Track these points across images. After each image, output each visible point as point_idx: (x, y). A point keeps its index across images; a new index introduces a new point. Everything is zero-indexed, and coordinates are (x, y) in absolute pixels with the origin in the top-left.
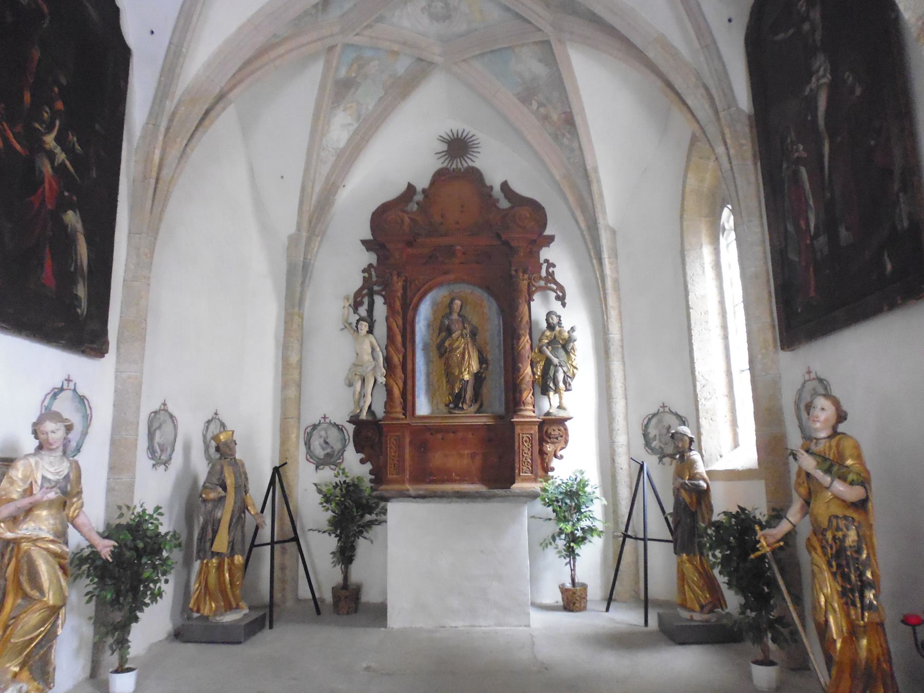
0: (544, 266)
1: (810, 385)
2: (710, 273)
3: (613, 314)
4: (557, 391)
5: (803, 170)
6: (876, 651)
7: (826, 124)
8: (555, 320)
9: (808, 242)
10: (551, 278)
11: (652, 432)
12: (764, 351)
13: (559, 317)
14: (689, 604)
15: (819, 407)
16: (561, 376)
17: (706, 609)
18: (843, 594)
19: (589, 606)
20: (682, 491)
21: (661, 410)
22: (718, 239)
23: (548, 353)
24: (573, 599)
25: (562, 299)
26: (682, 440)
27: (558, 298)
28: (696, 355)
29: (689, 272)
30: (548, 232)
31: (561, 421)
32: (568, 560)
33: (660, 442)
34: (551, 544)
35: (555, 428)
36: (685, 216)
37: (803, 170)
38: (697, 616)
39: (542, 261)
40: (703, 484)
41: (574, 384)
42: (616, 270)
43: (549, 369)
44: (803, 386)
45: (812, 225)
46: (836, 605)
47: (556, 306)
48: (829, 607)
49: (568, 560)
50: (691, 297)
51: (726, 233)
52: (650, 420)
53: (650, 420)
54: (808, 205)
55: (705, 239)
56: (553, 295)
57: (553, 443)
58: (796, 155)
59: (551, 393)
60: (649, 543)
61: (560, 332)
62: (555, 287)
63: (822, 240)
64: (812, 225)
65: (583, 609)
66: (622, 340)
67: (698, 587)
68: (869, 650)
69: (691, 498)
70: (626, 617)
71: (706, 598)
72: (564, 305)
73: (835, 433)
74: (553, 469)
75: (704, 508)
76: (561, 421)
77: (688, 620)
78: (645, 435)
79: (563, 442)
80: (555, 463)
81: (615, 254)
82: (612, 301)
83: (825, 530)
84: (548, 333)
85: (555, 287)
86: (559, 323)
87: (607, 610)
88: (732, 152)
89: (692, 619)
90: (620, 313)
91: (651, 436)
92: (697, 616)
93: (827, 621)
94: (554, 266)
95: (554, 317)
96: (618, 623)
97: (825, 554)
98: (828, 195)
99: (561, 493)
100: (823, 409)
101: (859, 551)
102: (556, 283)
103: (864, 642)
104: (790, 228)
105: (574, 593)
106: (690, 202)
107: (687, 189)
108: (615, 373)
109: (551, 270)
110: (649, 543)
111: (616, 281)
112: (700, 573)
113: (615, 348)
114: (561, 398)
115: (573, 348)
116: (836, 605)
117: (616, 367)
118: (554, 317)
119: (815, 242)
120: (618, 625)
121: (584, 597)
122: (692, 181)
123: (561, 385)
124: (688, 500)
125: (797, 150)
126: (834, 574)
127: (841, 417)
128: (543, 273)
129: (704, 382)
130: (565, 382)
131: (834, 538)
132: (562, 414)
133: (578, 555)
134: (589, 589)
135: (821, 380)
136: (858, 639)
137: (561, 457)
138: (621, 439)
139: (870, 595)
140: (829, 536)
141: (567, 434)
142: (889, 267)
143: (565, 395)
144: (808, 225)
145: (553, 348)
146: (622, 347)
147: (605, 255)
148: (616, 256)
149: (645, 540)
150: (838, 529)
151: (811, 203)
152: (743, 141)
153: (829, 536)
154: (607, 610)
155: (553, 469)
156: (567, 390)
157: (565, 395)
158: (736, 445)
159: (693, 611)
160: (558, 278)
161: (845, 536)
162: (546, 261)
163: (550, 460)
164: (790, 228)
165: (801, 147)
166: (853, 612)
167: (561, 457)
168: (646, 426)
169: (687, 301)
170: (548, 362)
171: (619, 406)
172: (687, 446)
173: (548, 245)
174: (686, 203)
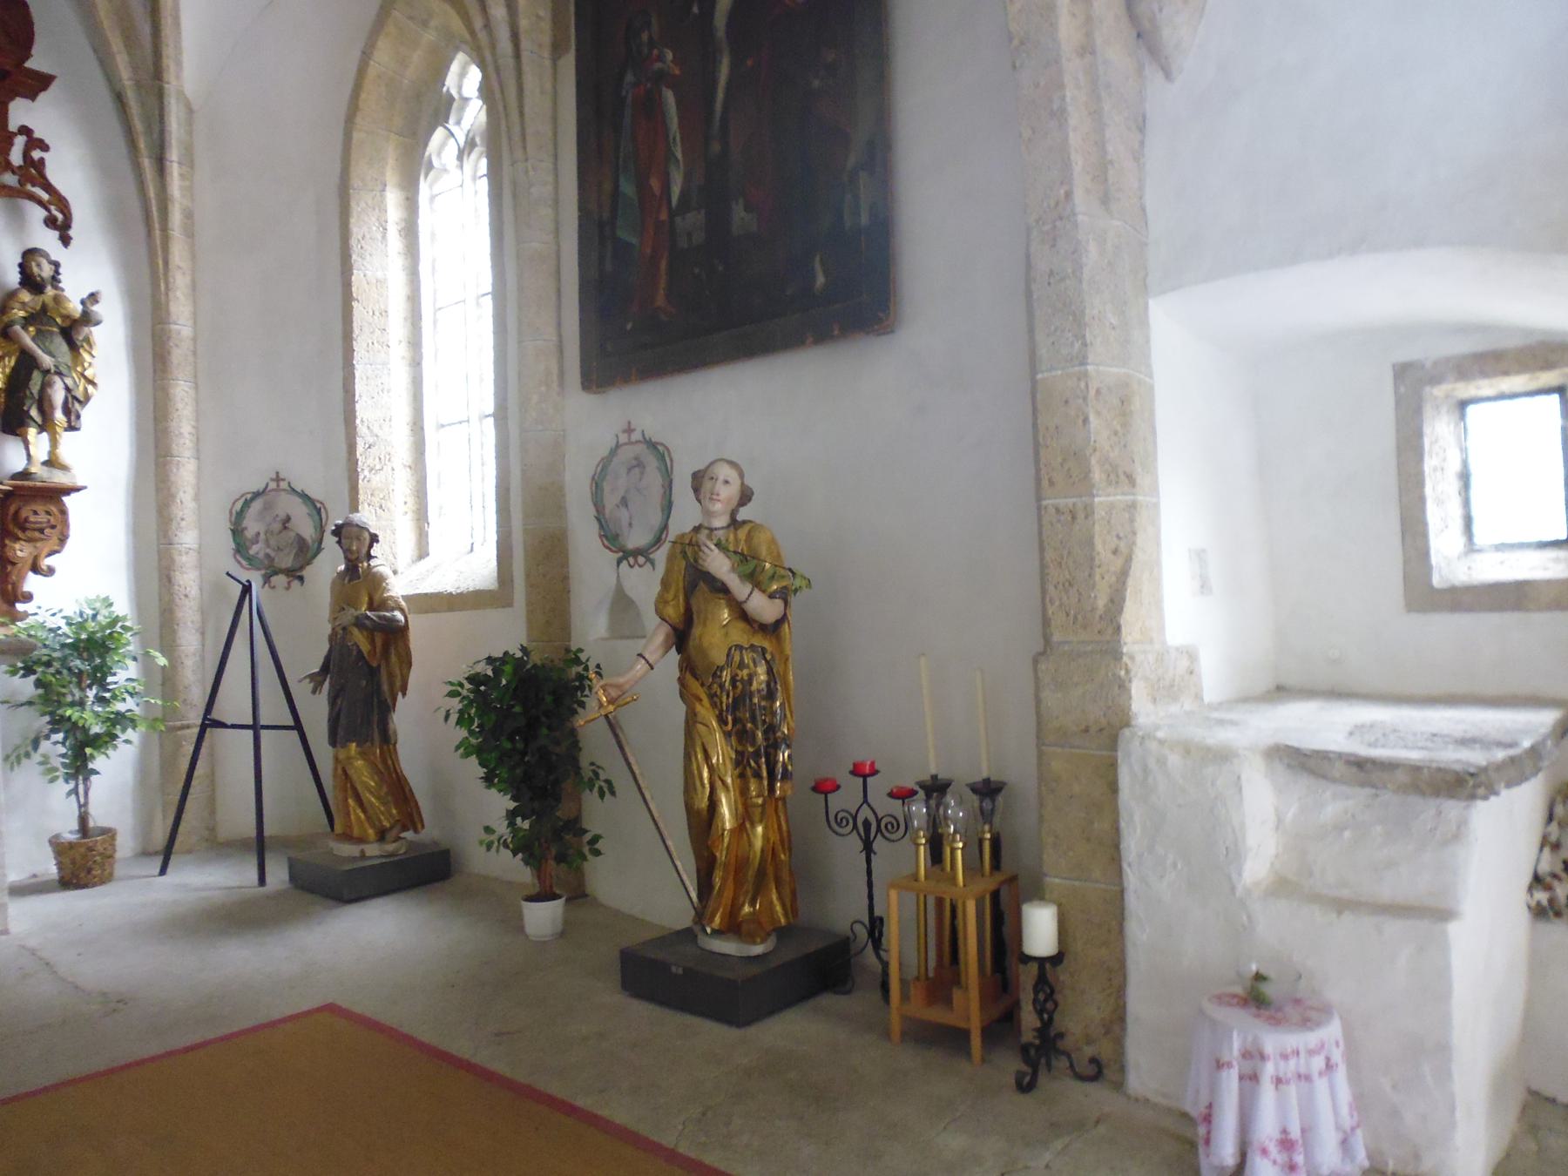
0: (20, 141)
1: (627, 454)
2: (395, 242)
3: (180, 281)
4: (46, 425)
5: (669, 97)
6: (774, 837)
7: (729, 25)
8: (47, 271)
9: (664, 216)
10: (34, 171)
11: (252, 526)
12: (543, 389)
13: (57, 265)
14: (356, 832)
15: (721, 478)
16: (58, 395)
17: (390, 836)
18: (740, 761)
19: (119, 870)
20: (356, 631)
21: (273, 485)
22: (418, 180)
23: (28, 341)
24: (81, 862)
25: (62, 227)
26: (358, 539)
27: (50, 222)
28: (359, 387)
29: (356, 230)
30: (35, 63)
31: (55, 495)
32: (72, 785)
33: (268, 546)
34: (28, 755)
35: (40, 508)
36: (358, 120)
37: (669, 97)
38: (373, 849)
39: (13, 126)
40: (398, 615)
41: (87, 414)
42: (189, 191)
43: (28, 378)
44: (614, 451)
45: (676, 191)
46: (729, 781)
47: (47, 240)
48: (718, 784)
49: (72, 785)
50: (357, 277)
51: (432, 174)
52: (247, 504)
53: (247, 504)
54: (669, 155)
55: (391, 177)
56: (38, 213)
57: (29, 540)
58: (658, 65)
59: (32, 432)
60: (263, 733)
61: (58, 300)
62: (45, 196)
63: (693, 220)
64: (676, 191)
65: (105, 880)
66: (195, 339)
67: (378, 798)
68: (765, 837)
69: (373, 642)
70: (226, 878)
71: (391, 815)
72: (66, 240)
73: (734, 524)
74: (28, 597)
75: (394, 659)
76: (55, 495)
77: (354, 859)
78: (237, 532)
79: (55, 539)
80: (32, 583)
81: (189, 161)
82: (179, 252)
83: (721, 669)
84: (26, 296)
85: (45, 196)
86: (55, 279)
87: (163, 872)
88: (524, 23)
89: (363, 856)
90: (194, 286)
91: (249, 534)
92: (373, 849)
93: (713, 804)
94: (44, 147)
95: (44, 262)
96: (196, 890)
97: (714, 705)
98: (716, 147)
99: (63, 646)
100: (727, 482)
101: (770, 695)
102: (48, 187)
103: (760, 829)
104: (628, 188)
105: (91, 849)
106: (371, 99)
107: (373, 70)
108: (180, 406)
109: (36, 154)
110: (263, 733)
111: (189, 215)
112: (379, 773)
113: (179, 355)
114: (54, 443)
115: (87, 340)
116: (729, 781)
117: (182, 392)
118: (44, 262)
119: (678, 220)
120: (204, 894)
121: (109, 857)
122: (383, 55)
123: (59, 415)
124: (365, 647)
125: (661, 58)
126: (727, 735)
127: (745, 497)
128: (16, 157)
129: (371, 440)
130: (67, 411)
131: (734, 681)
132: (59, 478)
133: (96, 772)
134: (119, 840)
135: (652, 445)
136: (753, 826)
137: (50, 571)
138: (187, 538)
139: (783, 755)
140: (726, 675)
141: (65, 523)
142: (821, 280)
143: (66, 438)
144: (666, 187)
145: (39, 332)
146: (195, 353)
147: (173, 155)
148: (192, 166)
149: (256, 727)
150: (742, 665)
151: (679, 155)
152: (542, 13)
153: (726, 675)
154: (163, 872)
155: (28, 597)
156: (71, 428)
157: (66, 438)
158: (422, 553)
159: (361, 840)
160: (53, 174)
161: (751, 677)
162: (25, 130)
163: (22, 578)
164: (628, 188)
165: (669, 56)
166: (753, 787)
167: (50, 571)
168: (241, 515)
169: (347, 285)
170: (27, 363)
171: (185, 474)
172: (364, 550)
173: (32, 96)
174: (363, 96)
